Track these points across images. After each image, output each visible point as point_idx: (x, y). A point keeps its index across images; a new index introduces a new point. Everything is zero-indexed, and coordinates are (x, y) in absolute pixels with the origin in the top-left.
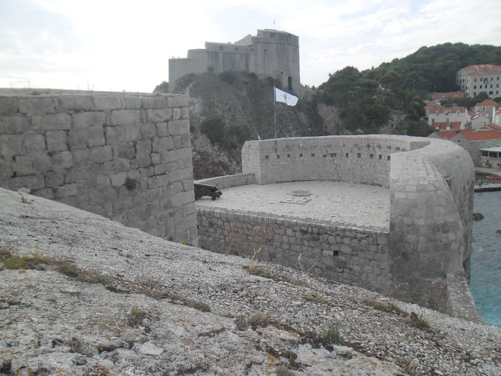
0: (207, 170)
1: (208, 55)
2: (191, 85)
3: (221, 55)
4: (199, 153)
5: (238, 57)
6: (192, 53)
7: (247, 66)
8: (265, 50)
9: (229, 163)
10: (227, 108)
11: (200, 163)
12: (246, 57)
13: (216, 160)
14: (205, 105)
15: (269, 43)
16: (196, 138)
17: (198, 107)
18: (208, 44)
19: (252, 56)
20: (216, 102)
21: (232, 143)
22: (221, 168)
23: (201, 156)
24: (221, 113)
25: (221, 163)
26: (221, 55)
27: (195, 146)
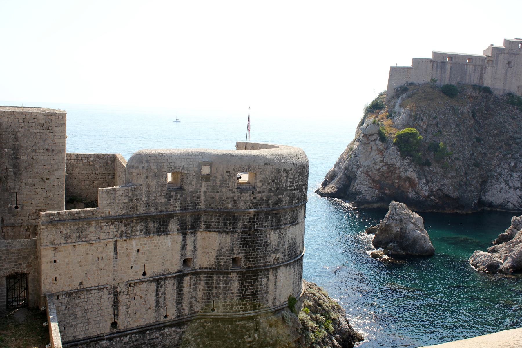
0: (393, 184)
1: (433, 66)
2: (404, 95)
3: (449, 66)
4: (386, 165)
5: (470, 68)
6: (417, 62)
7: (481, 79)
8: (509, 63)
9: (417, 180)
10: (434, 122)
11: (386, 175)
12: (482, 69)
13: (403, 175)
14: (410, 116)
15: (517, 54)
16: (387, 149)
17: (402, 118)
18: (435, 54)
19: (489, 68)
20: (422, 116)
21: (427, 160)
22: (407, 183)
23: (388, 168)
24: (425, 127)
25: (409, 180)
26: (449, 66)
27: (384, 157)
